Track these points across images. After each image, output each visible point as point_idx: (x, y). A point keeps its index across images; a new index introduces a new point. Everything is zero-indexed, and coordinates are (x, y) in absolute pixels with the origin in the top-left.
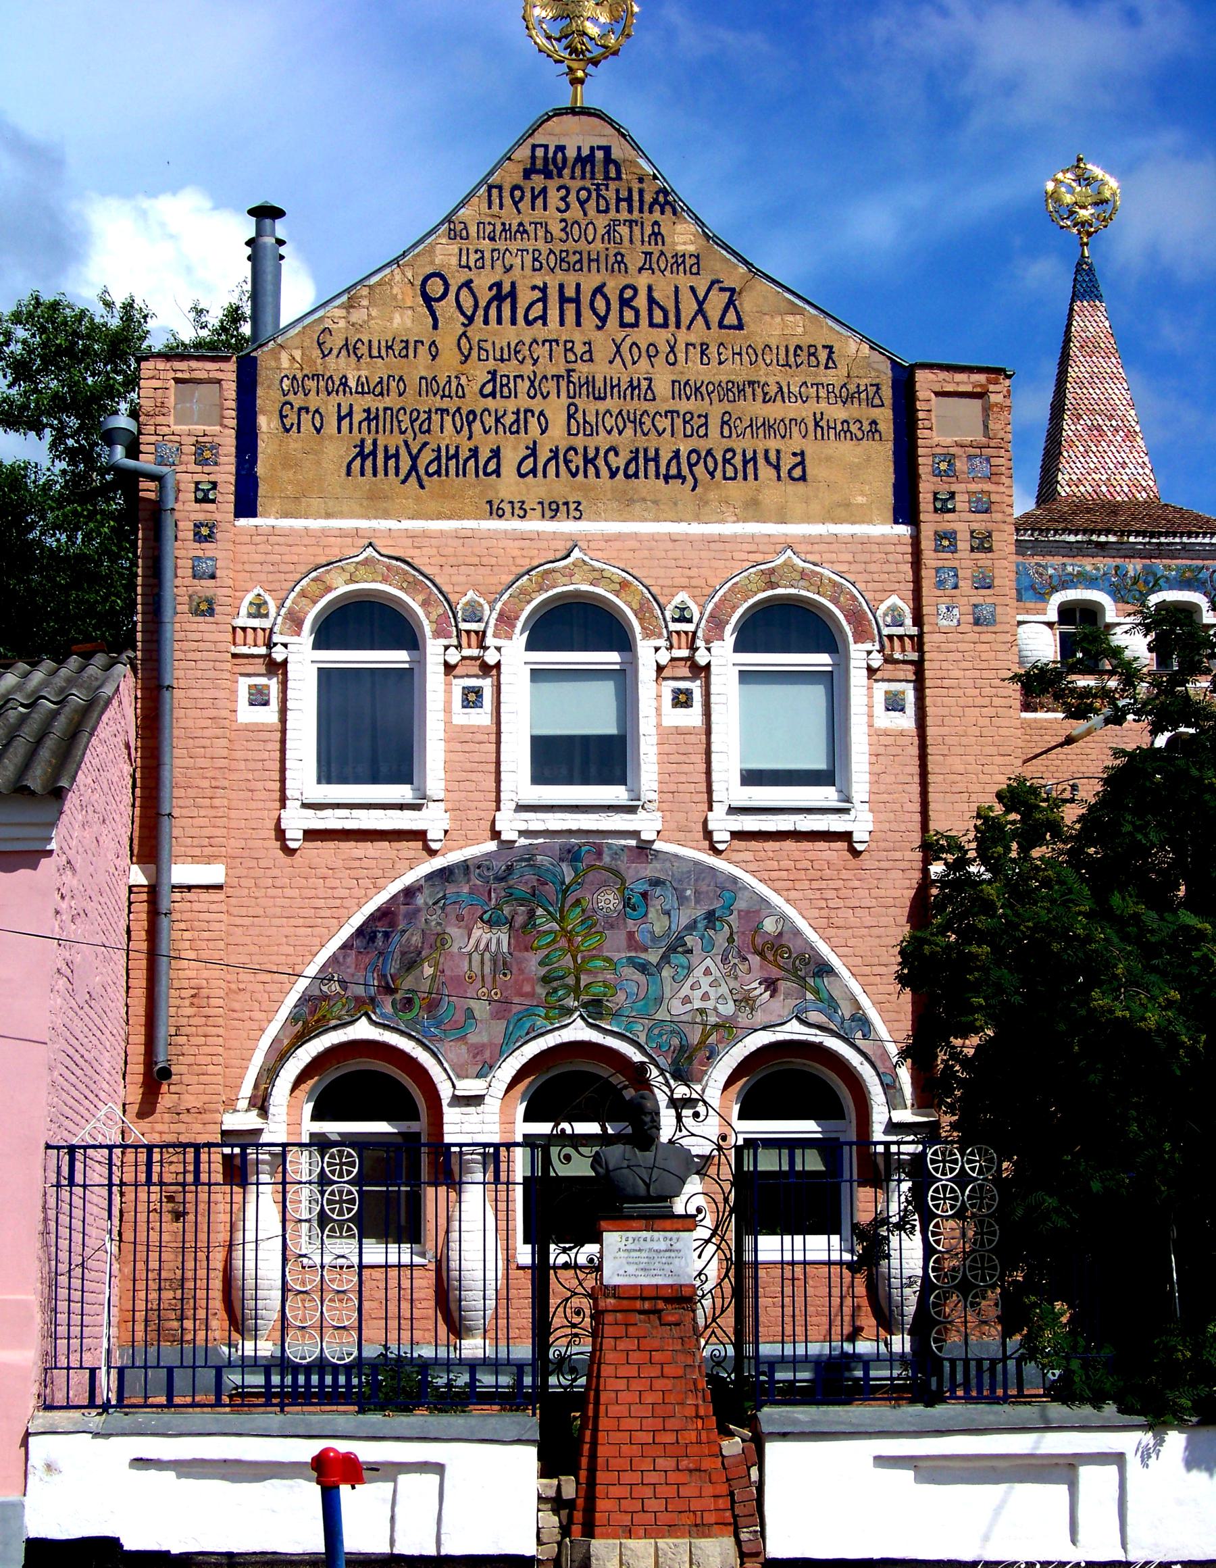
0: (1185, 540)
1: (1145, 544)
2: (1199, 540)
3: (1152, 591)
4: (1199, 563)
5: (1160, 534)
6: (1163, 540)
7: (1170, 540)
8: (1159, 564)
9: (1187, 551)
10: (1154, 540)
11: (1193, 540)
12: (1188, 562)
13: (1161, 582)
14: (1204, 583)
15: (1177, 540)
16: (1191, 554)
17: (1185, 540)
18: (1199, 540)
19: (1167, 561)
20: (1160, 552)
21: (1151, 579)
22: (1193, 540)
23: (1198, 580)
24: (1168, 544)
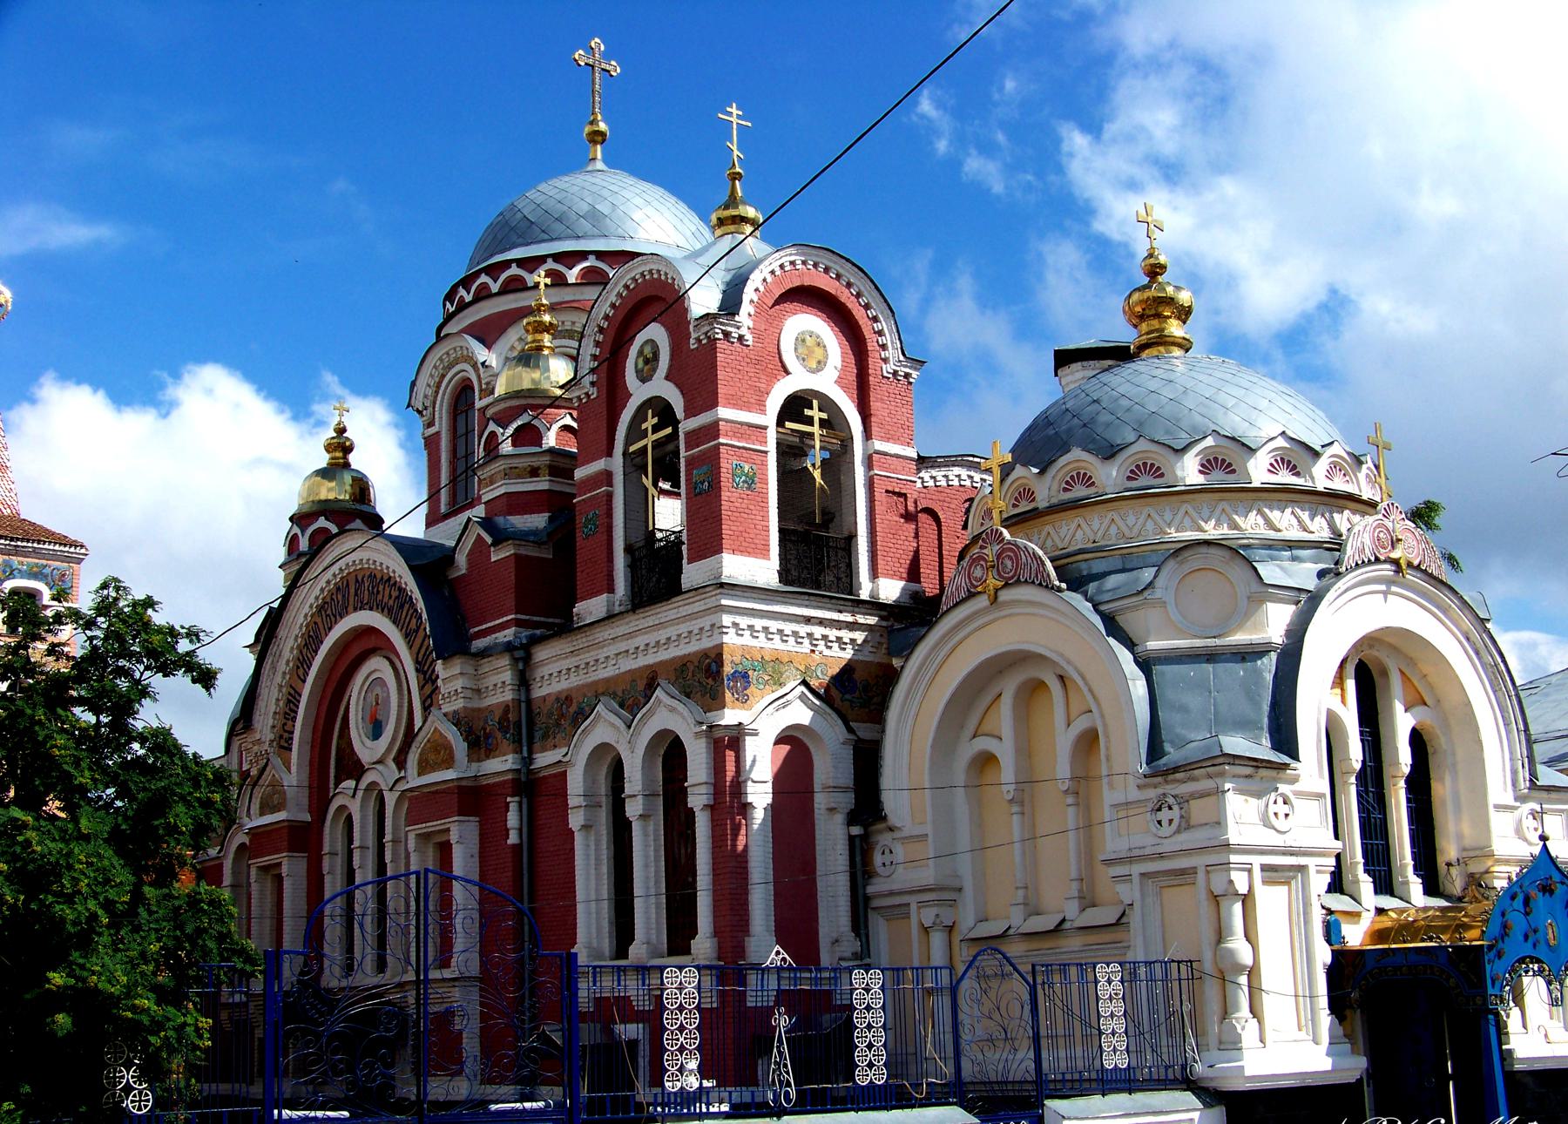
0: (35, 545)
1: (6, 545)
2: (46, 546)
3: (8, 578)
4: (44, 562)
5: (18, 539)
6: (19, 543)
7: (25, 544)
8: (15, 560)
9: (36, 553)
10: (13, 543)
11: (41, 546)
12: (37, 561)
13: (15, 572)
14: (46, 576)
15: (30, 545)
16: (39, 556)
17: (35, 545)
18: (46, 546)
19: (21, 559)
20: (17, 552)
21: (8, 569)
22: (41, 546)
23: (41, 573)
24: (23, 547)
